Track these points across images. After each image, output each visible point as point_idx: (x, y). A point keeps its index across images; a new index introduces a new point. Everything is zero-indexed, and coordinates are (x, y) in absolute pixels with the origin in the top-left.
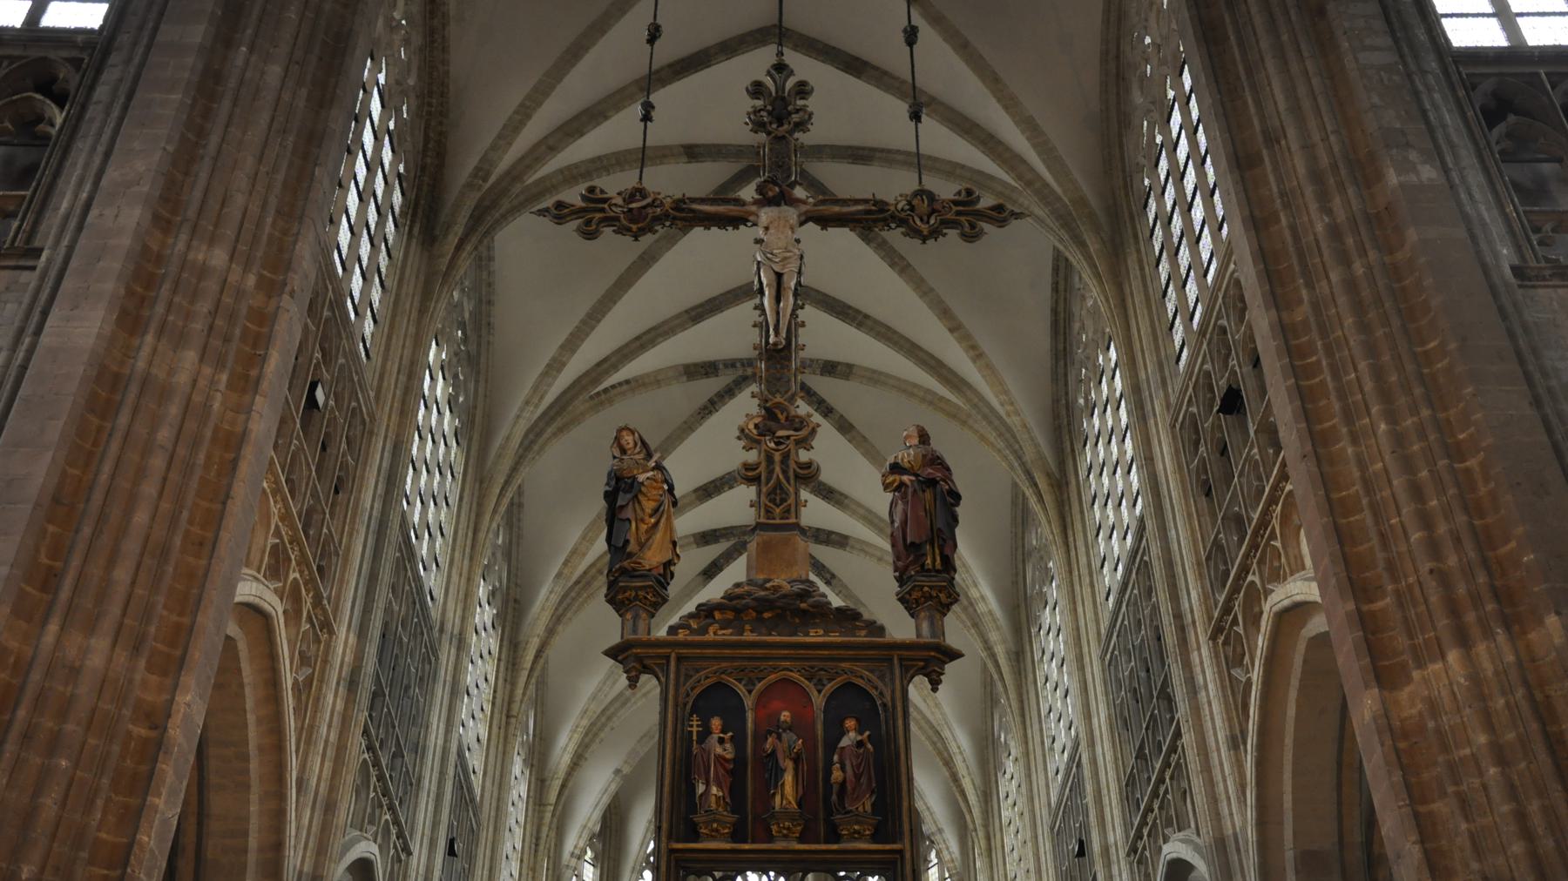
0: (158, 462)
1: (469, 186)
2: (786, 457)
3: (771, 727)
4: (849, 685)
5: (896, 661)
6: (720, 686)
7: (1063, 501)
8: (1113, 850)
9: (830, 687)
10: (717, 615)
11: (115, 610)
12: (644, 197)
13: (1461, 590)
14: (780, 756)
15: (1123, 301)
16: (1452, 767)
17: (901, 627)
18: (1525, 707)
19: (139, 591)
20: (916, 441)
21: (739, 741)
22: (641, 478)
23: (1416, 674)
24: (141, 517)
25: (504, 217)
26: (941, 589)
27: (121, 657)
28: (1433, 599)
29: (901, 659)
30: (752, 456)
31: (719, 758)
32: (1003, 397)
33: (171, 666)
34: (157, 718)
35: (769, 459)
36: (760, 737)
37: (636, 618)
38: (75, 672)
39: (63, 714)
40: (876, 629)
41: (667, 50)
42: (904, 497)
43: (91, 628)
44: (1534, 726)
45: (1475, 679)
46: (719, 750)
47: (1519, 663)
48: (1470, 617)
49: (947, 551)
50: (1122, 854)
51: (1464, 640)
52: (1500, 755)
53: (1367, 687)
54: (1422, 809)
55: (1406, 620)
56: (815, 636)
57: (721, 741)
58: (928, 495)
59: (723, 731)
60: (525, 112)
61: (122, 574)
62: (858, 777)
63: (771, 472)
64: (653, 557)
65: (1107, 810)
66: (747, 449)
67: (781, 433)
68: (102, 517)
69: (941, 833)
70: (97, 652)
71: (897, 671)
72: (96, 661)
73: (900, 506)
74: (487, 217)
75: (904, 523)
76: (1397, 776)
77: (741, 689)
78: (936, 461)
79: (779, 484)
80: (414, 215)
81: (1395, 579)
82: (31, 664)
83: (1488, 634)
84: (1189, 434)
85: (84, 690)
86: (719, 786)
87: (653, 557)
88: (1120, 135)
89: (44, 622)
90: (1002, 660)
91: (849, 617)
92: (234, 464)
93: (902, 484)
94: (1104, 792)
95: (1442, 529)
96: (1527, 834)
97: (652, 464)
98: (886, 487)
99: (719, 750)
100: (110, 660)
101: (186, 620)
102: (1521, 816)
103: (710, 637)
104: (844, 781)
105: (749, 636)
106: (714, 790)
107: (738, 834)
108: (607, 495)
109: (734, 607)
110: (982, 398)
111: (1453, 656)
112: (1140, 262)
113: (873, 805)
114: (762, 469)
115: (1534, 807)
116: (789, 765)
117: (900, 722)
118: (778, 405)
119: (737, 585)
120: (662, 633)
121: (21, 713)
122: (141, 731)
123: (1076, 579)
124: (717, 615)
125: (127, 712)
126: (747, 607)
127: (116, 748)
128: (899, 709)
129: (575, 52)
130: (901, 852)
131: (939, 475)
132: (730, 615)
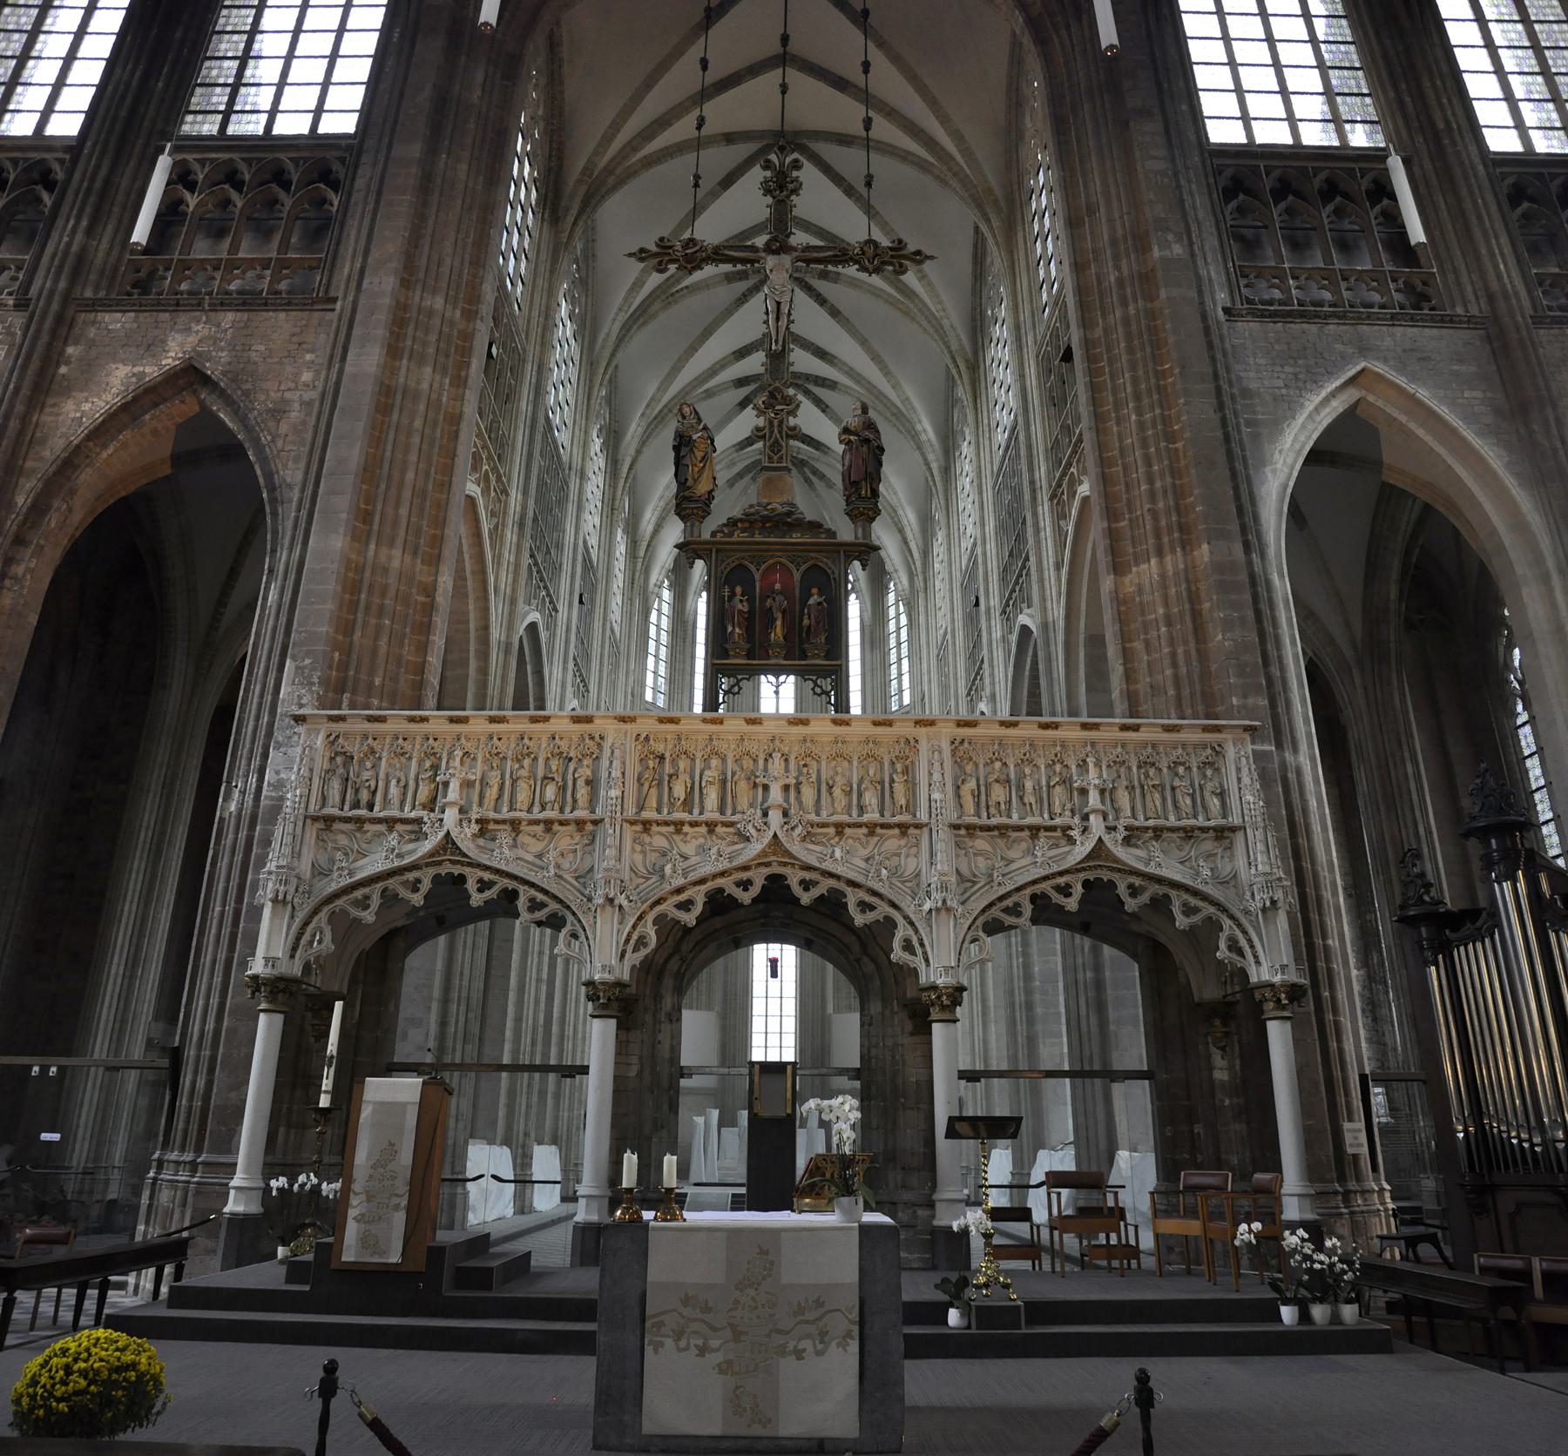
0: (416, 440)
1: (579, 181)
2: (781, 422)
3: (768, 593)
4: (815, 566)
6: (741, 566)
9: (803, 568)
10: (739, 525)
11: (402, 533)
12: (695, 245)
13: (1163, 523)
14: (774, 610)
15: (1013, 264)
16: (1145, 625)
17: (846, 532)
18: (1184, 594)
19: (413, 519)
20: (859, 412)
21: (751, 601)
22: (695, 437)
23: (1134, 569)
24: (410, 476)
25: (603, 197)
26: (870, 509)
27: (408, 558)
28: (1148, 527)
30: (761, 422)
31: (740, 612)
32: (939, 307)
33: (435, 560)
34: (430, 591)
35: (771, 423)
36: (764, 598)
37: (692, 526)
38: (386, 570)
39: (383, 595)
40: (831, 534)
41: (713, 75)
42: (851, 449)
43: (391, 544)
44: (1187, 606)
45: (1163, 576)
46: (740, 606)
47: (1186, 570)
48: (1166, 539)
51: (1160, 554)
52: (1169, 624)
53: (1108, 574)
54: (1127, 645)
55: (1133, 537)
56: (796, 538)
57: (741, 601)
58: (865, 449)
59: (742, 595)
60: (615, 127)
61: (403, 511)
62: (817, 623)
63: (772, 432)
64: (702, 488)
66: (758, 416)
67: (777, 408)
68: (390, 477)
70: (396, 558)
72: (396, 564)
73: (848, 457)
74: (595, 194)
75: (850, 466)
76: (1117, 627)
77: (753, 568)
78: (871, 426)
79: (776, 441)
80: (545, 205)
81: (1130, 512)
82: (364, 567)
83: (1173, 551)
84: (1045, 369)
85: (392, 581)
86: (740, 628)
87: (702, 488)
88: (1017, 146)
89: (367, 544)
91: (815, 526)
92: (457, 433)
93: (850, 441)
95: (1158, 484)
96: (1175, 665)
97: (701, 427)
98: (841, 442)
99: (740, 606)
100: (402, 561)
101: (439, 532)
102: (1173, 655)
103: (735, 539)
104: (809, 627)
105: (758, 538)
106: (737, 630)
107: (750, 655)
108: (675, 448)
109: (750, 521)
110: (925, 305)
111: (1153, 561)
112: (1025, 238)
114: (766, 430)
115: (1180, 651)
116: (779, 616)
118: (777, 389)
119: (751, 506)
120: (706, 536)
121: (363, 596)
122: (421, 599)
124: (739, 525)
125: (414, 590)
126: (756, 521)
127: (411, 611)
129: (650, 82)
130: (840, 666)
131: (872, 436)
132: (747, 525)
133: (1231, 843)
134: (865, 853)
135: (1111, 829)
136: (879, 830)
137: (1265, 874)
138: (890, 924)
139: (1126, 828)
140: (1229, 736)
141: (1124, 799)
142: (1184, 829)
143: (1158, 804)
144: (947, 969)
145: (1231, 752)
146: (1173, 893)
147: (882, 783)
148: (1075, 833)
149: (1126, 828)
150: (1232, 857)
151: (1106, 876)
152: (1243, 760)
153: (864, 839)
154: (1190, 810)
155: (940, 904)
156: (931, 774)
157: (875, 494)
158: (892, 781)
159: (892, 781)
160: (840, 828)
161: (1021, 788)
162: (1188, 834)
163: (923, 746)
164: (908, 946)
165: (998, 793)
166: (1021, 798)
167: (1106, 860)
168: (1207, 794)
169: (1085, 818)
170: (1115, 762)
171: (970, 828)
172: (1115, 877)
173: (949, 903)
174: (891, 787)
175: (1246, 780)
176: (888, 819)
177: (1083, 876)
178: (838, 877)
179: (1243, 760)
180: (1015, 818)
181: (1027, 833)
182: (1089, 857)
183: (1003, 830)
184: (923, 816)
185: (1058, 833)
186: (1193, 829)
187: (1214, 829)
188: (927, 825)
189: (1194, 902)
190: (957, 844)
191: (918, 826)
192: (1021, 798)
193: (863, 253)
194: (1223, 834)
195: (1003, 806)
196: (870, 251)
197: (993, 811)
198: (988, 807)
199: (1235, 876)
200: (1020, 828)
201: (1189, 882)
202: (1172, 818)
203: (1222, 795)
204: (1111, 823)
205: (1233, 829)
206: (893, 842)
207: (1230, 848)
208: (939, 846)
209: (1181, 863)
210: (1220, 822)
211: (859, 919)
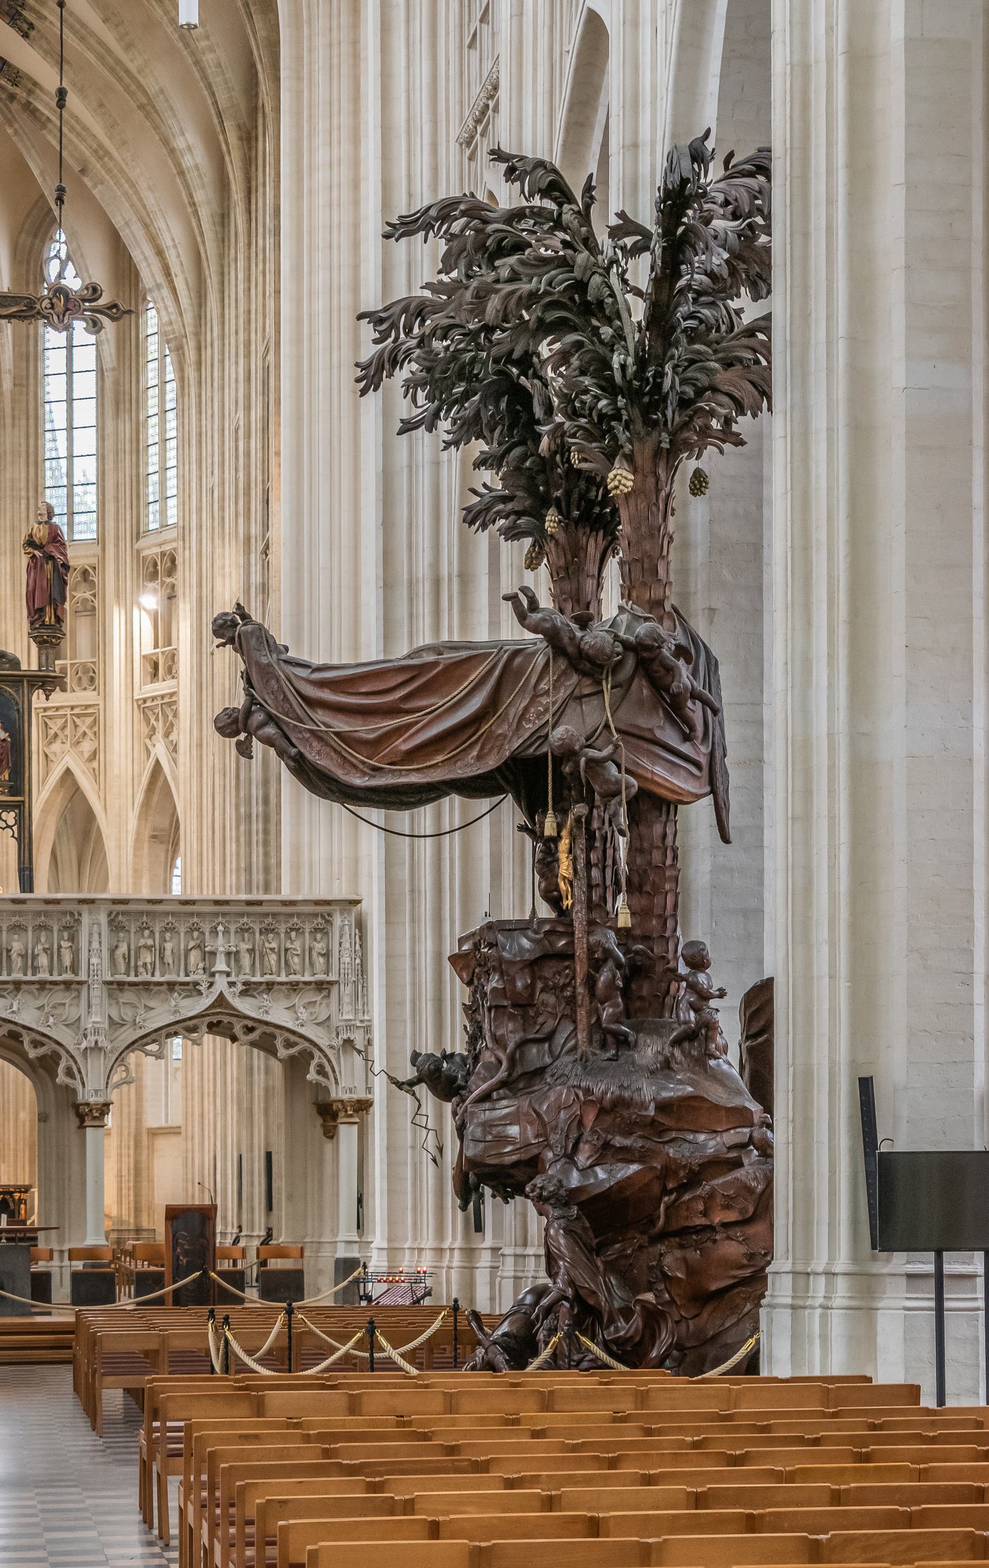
5: (25, 684)
7: (250, 158)
8: (253, 540)
29: (28, 681)
40: (15, 663)
49: (59, 613)
50: (259, 552)
65: (253, 503)
69: (159, 290)
71: (26, 691)
90: (206, 226)
93: (34, 556)
94: (253, 485)
113: (9, 774)
117: (26, 725)
123: (253, 255)
128: (26, 713)
130: (23, 802)
133: (329, 993)
134: (39, 1003)
135: (231, 984)
136: (48, 986)
137: (346, 1020)
138: (55, 1057)
139: (244, 984)
140: (337, 908)
141: (246, 960)
142: (290, 983)
143: (273, 962)
144: (96, 1091)
145: (337, 920)
146: (277, 1032)
147: (51, 949)
148: (203, 988)
149: (244, 984)
150: (328, 1005)
151: (226, 1019)
152: (347, 928)
153: (36, 993)
154: (297, 968)
155: (93, 1045)
156: (90, 943)
157: (59, 620)
158: (60, 947)
159: (60, 947)
160: (18, 985)
161: (162, 951)
162: (294, 987)
163: (86, 919)
164: (69, 1073)
165: (147, 957)
166: (162, 958)
167: (226, 1008)
168: (314, 954)
169: (213, 975)
170: (241, 929)
171: (121, 984)
172: (233, 1020)
173: (100, 1045)
174: (59, 951)
175: (346, 945)
176: (56, 978)
177: (208, 1020)
178: (16, 1024)
179: (347, 928)
180: (158, 978)
181: (164, 988)
182: (212, 1006)
183: (146, 985)
184: (83, 977)
185: (191, 987)
186: (297, 983)
187: (316, 983)
188: (86, 982)
189: (293, 1038)
190: (110, 996)
191: (80, 983)
192: (162, 958)
193: (52, 307)
194: (322, 987)
195: (149, 966)
196: (60, 304)
197: (141, 970)
198: (136, 967)
199: (329, 1017)
200: (160, 984)
201: (290, 1025)
202: (283, 973)
203: (327, 955)
204: (232, 979)
205: (331, 983)
206: (60, 996)
207: (328, 996)
208: (95, 1001)
209: (287, 1008)
210: (321, 977)
211: (32, 1054)
